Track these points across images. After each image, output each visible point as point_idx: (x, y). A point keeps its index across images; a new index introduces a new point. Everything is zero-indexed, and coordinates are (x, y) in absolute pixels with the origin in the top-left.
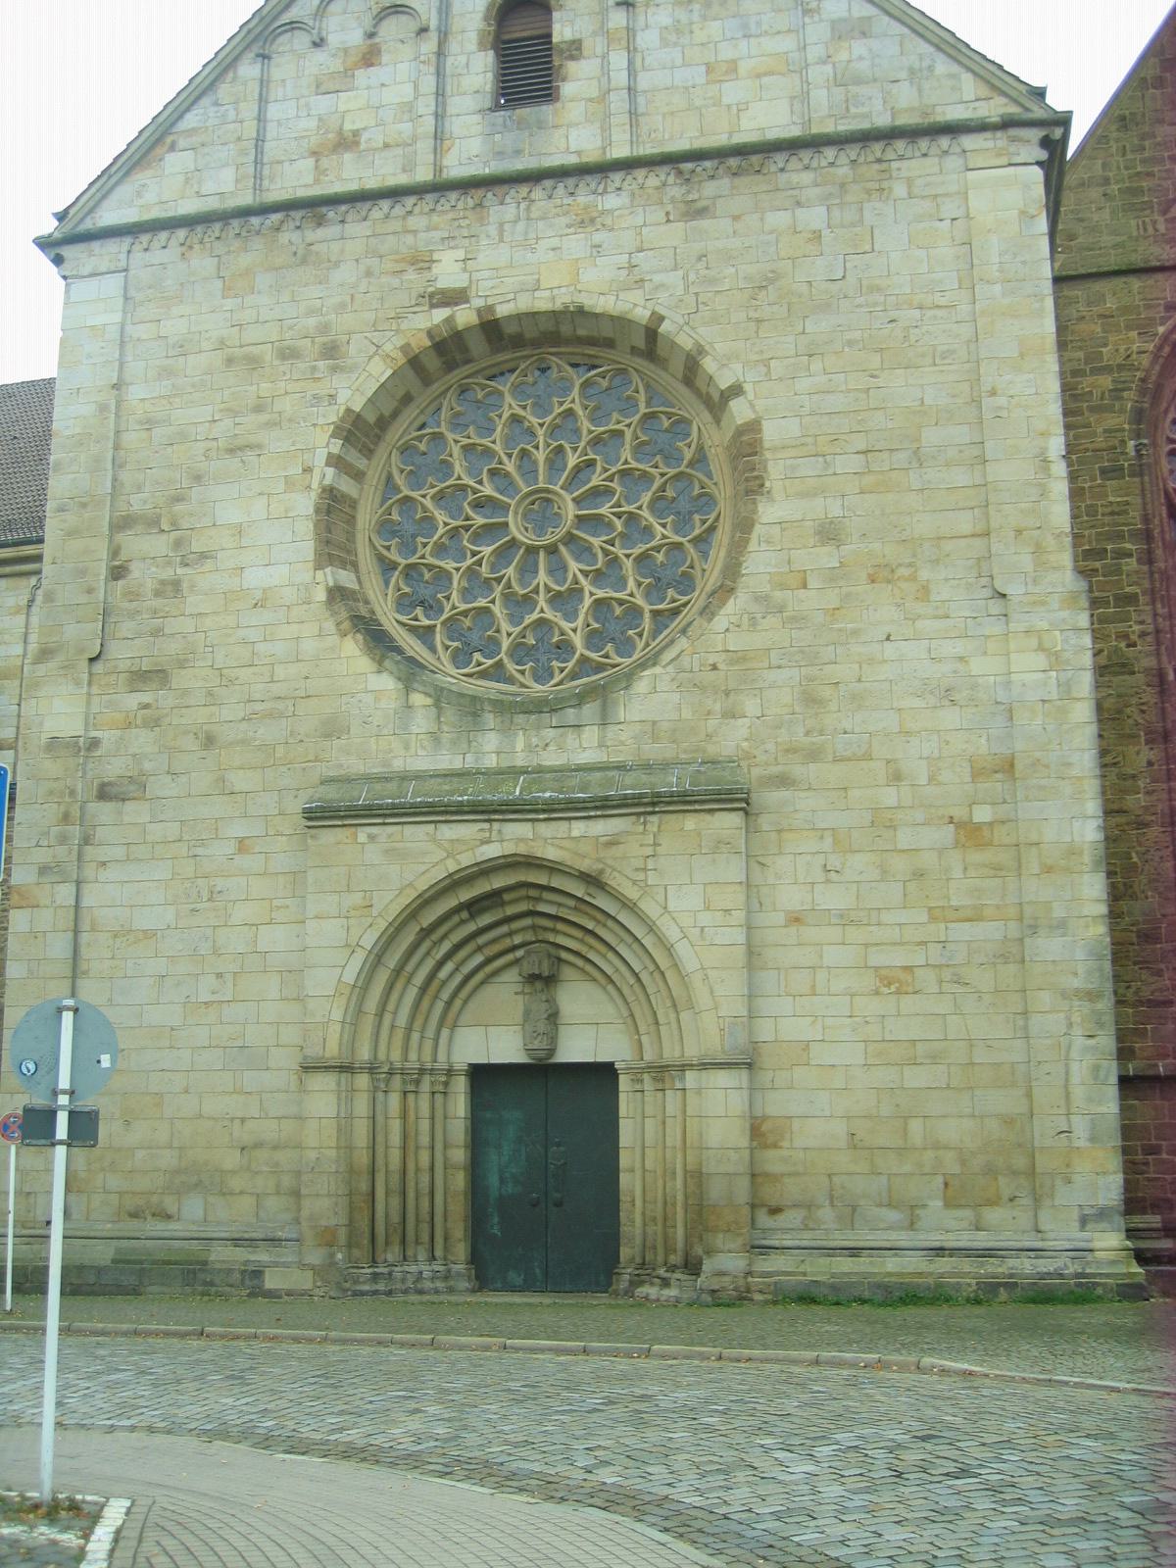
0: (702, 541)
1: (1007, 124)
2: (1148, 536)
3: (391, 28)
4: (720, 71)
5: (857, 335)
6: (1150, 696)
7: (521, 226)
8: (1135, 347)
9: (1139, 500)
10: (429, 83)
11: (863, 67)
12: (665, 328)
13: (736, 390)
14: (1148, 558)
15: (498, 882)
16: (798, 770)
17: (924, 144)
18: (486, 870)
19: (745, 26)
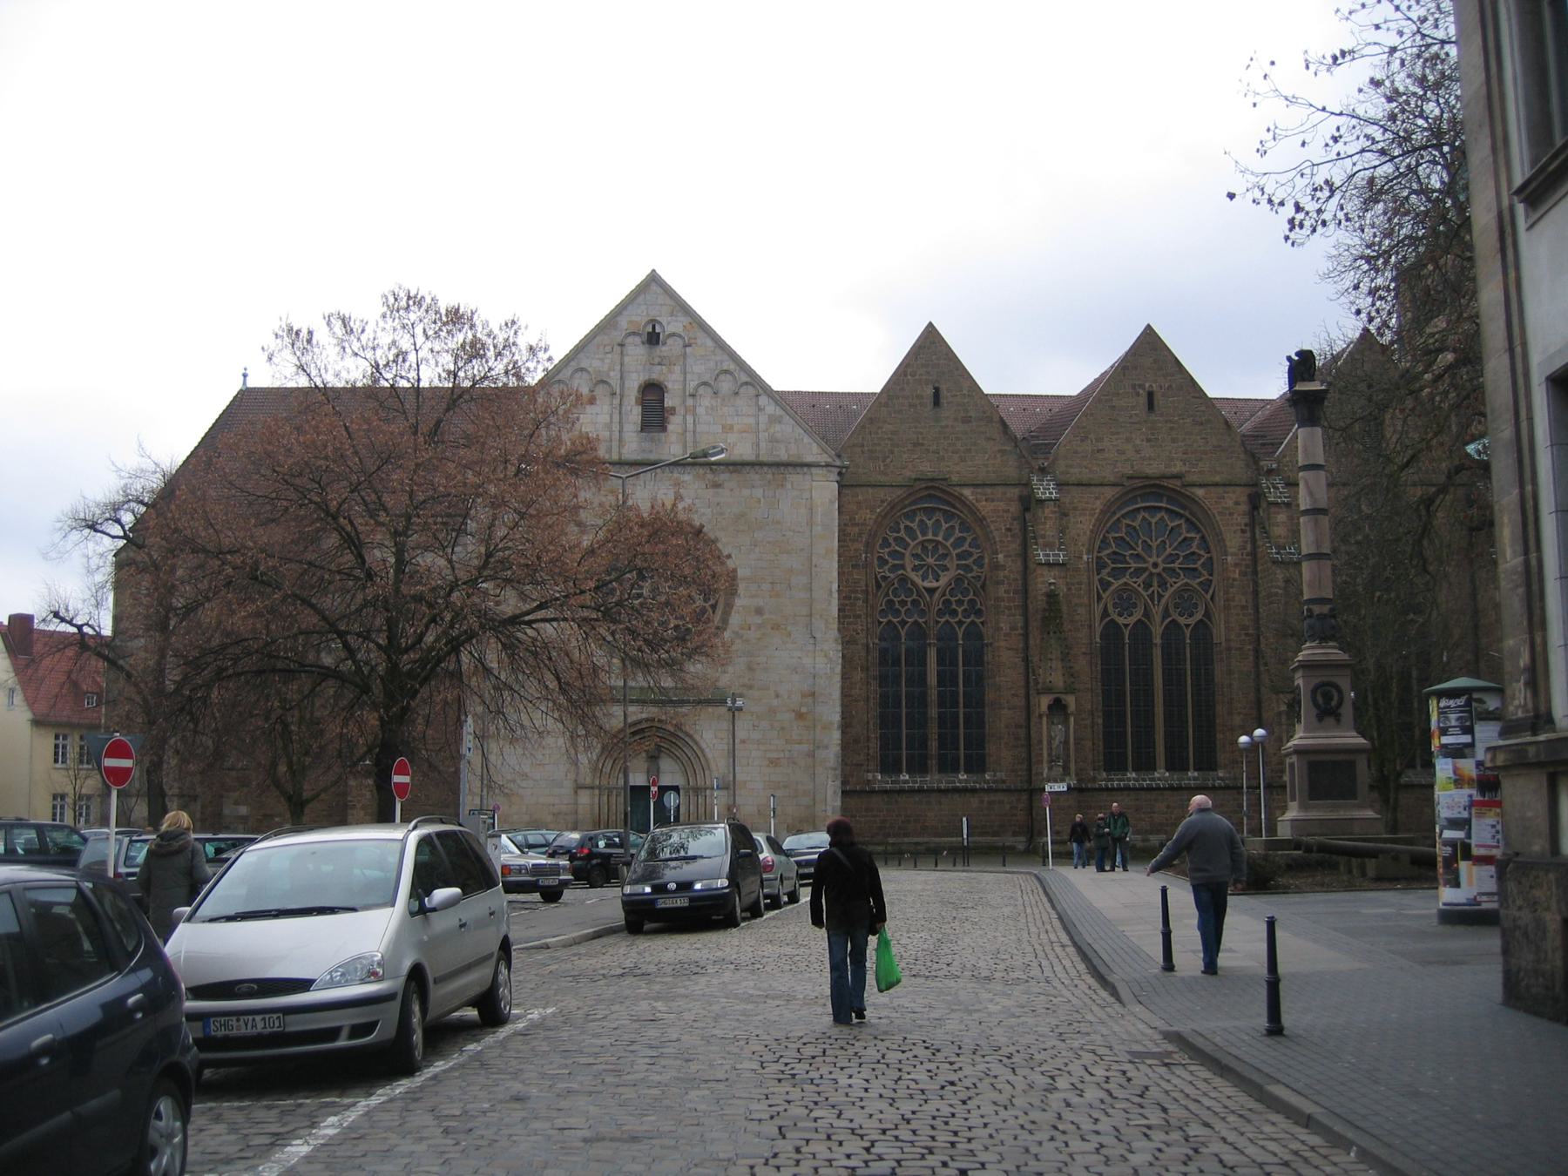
0: (714, 607)
1: (827, 465)
2: (866, 592)
3: (600, 391)
4: (728, 429)
5: (771, 539)
6: (863, 654)
7: (652, 483)
8: (868, 516)
9: (864, 578)
10: (616, 418)
11: (779, 435)
12: (705, 530)
13: (729, 556)
14: (866, 601)
15: (644, 725)
16: (745, 692)
17: (798, 469)
18: (640, 722)
19: (737, 411)
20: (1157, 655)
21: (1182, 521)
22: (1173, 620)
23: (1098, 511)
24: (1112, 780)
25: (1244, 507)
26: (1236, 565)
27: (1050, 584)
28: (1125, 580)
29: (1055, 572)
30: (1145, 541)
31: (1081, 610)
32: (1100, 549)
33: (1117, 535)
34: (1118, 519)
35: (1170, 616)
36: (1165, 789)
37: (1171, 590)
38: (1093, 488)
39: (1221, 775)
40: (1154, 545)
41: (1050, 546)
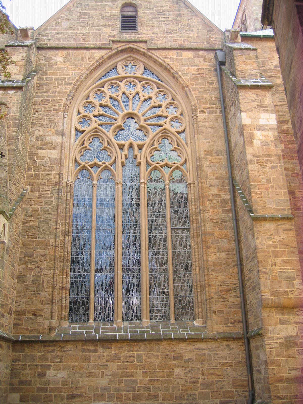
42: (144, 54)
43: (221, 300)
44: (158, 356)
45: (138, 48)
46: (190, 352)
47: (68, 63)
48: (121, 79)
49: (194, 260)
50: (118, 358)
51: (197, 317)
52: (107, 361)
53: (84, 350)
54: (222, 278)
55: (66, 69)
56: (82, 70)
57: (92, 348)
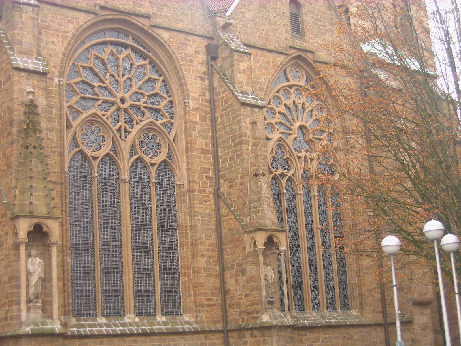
20: (125, 190)
21: (147, 62)
22: (140, 157)
23: (70, 35)
24: (83, 326)
25: (203, 57)
26: (197, 109)
27: (28, 93)
28: (93, 111)
29: (35, 80)
30: (112, 76)
31: (53, 136)
32: (70, 77)
33: (86, 65)
34: (87, 49)
35: (136, 153)
36: (138, 335)
37: (137, 128)
38: (65, 11)
39: (187, 319)
40: (122, 80)
41: (27, 53)
42: (308, 64)
43: (371, 296)
44: (340, 337)
45: (307, 58)
46: (356, 334)
47: (258, 65)
48: (291, 87)
49: (349, 264)
50: (318, 339)
51: (353, 308)
52: (312, 342)
53: (298, 335)
54: (370, 279)
55: (257, 71)
56: (269, 74)
57: (303, 333)
